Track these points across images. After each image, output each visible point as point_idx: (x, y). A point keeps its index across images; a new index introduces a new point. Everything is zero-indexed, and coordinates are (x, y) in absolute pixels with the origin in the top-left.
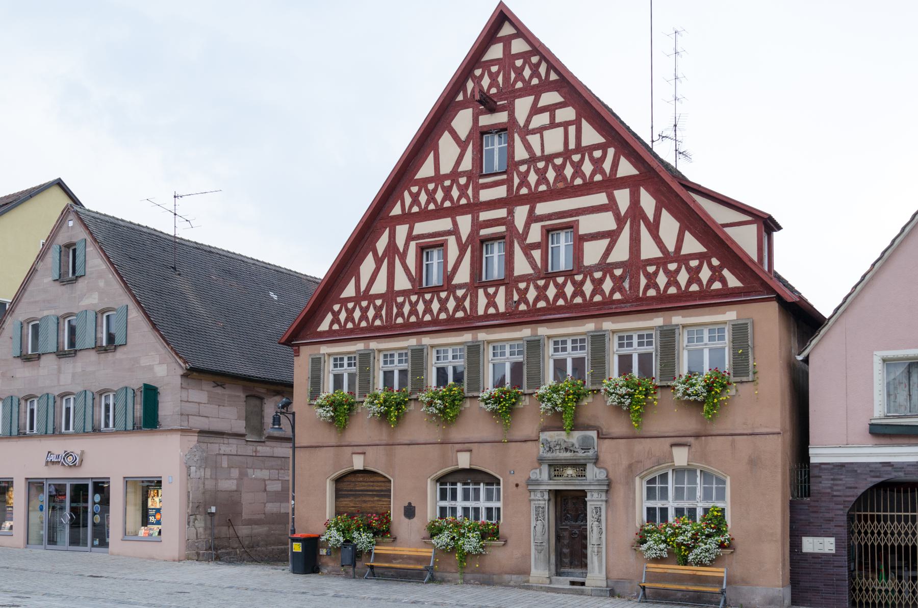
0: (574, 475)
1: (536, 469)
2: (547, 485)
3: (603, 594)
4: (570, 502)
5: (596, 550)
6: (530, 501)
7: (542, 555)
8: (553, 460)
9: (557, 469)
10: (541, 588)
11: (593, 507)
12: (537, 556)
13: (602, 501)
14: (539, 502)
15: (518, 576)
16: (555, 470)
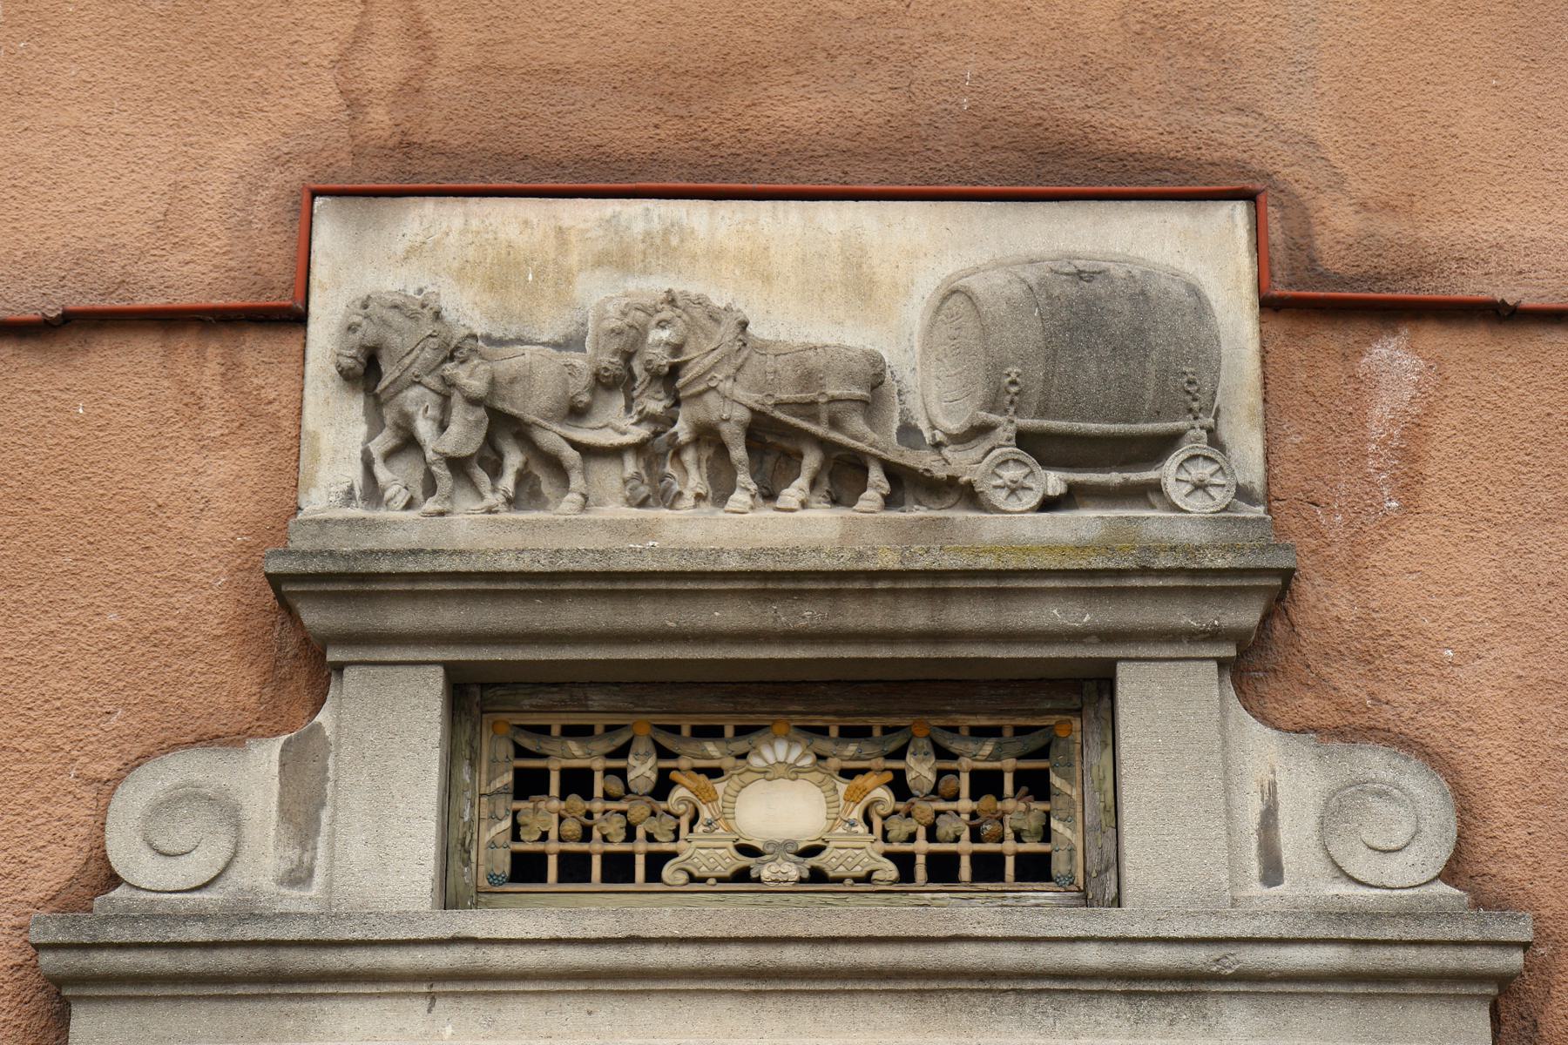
9: (576, 755)
16: (529, 784)
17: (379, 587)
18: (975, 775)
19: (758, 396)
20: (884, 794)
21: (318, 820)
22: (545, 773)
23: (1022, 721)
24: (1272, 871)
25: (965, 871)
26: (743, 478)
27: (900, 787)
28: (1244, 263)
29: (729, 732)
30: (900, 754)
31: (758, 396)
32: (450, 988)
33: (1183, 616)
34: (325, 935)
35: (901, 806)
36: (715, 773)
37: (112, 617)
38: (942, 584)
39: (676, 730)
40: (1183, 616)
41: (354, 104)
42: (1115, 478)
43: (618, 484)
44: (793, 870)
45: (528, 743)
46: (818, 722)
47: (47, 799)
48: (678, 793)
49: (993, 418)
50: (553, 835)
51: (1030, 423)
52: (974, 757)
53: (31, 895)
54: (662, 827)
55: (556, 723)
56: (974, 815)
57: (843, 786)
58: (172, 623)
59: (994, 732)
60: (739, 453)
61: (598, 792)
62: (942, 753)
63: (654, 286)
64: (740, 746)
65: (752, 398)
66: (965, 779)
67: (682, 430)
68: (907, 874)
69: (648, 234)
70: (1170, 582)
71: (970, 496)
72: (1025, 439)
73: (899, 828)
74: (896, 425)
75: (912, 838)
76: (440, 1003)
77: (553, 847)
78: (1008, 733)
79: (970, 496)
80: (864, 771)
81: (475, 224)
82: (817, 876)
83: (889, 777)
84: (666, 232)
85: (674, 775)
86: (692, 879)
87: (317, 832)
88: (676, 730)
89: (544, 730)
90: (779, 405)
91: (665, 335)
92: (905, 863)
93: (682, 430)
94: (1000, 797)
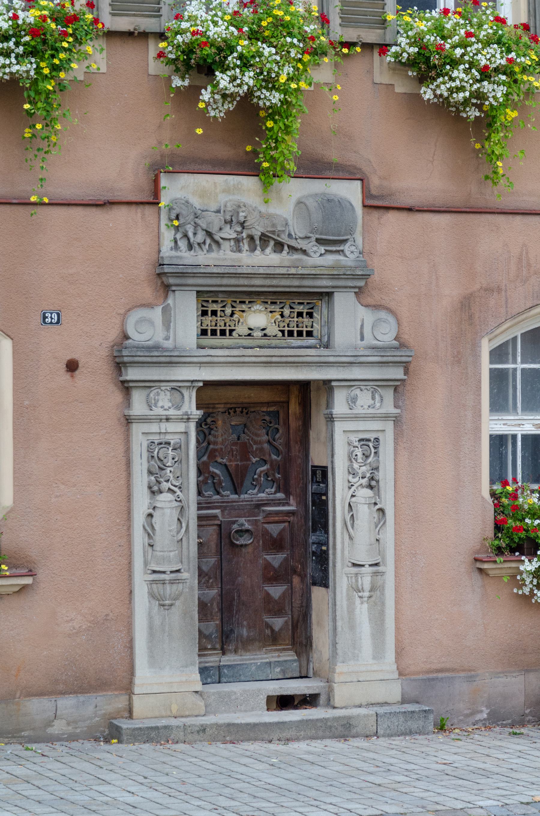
0: (273, 330)
1: (150, 306)
2: (201, 364)
3: (414, 725)
4: (220, 422)
5: (366, 582)
6: (128, 421)
7: (176, 613)
8: (221, 275)
9: (215, 307)
10: (203, 729)
11: (354, 438)
12: (157, 622)
13: (385, 417)
14: (165, 426)
15: (81, 698)
17: (187, 275)
18: (298, 313)
19: (263, 229)
20: (279, 317)
21: (170, 326)
22: (207, 311)
23: (309, 301)
24: (362, 339)
25: (295, 334)
26: (258, 248)
27: (282, 316)
28: (360, 196)
29: (247, 302)
30: (282, 308)
31: (263, 229)
32: (204, 365)
33: (350, 283)
34: (182, 355)
35: (282, 319)
36: (243, 311)
37: (121, 276)
38: (303, 276)
39: (235, 302)
40: (350, 283)
41: (160, 143)
42: (334, 248)
43: (228, 246)
44: (260, 334)
45: (205, 304)
46: (266, 300)
47: (110, 318)
48: (236, 316)
49: (311, 235)
50: (209, 325)
51: (318, 236)
52: (298, 309)
53: (109, 340)
54: (232, 324)
55: (210, 300)
56: (297, 322)
57: (270, 315)
58: (133, 277)
59: (303, 303)
60: (258, 242)
61: (219, 315)
62: (291, 308)
63: (237, 197)
64: (250, 306)
65: (262, 230)
66: (296, 313)
67: (244, 235)
68: (283, 335)
69: (234, 185)
70: (349, 277)
71: (304, 252)
72: (318, 240)
73: (282, 324)
74: (287, 234)
75: (284, 327)
76: (202, 368)
77: (209, 328)
78: (305, 304)
79: (304, 252)
80: (274, 311)
81: (196, 181)
82: (265, 335)
83: (280, 313)
84: (238, 184)
85: (235, 312)
86: (239, 336)
87: (170, 328)
88: (235, 302)
89: (208, 301)
90: (267, 231)
91: (244, 214)
92: (283, 332)
93: (244, 235)
94: (303, 318)
